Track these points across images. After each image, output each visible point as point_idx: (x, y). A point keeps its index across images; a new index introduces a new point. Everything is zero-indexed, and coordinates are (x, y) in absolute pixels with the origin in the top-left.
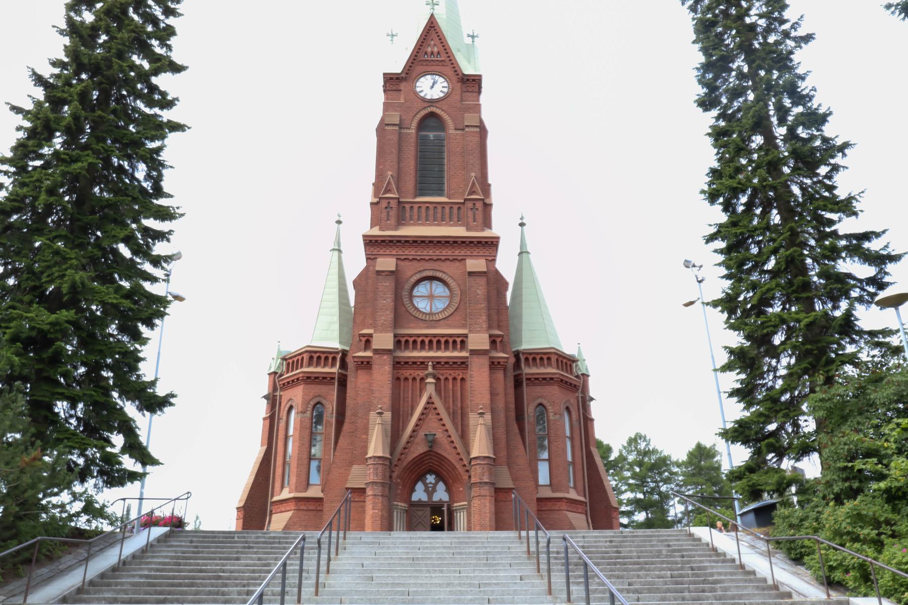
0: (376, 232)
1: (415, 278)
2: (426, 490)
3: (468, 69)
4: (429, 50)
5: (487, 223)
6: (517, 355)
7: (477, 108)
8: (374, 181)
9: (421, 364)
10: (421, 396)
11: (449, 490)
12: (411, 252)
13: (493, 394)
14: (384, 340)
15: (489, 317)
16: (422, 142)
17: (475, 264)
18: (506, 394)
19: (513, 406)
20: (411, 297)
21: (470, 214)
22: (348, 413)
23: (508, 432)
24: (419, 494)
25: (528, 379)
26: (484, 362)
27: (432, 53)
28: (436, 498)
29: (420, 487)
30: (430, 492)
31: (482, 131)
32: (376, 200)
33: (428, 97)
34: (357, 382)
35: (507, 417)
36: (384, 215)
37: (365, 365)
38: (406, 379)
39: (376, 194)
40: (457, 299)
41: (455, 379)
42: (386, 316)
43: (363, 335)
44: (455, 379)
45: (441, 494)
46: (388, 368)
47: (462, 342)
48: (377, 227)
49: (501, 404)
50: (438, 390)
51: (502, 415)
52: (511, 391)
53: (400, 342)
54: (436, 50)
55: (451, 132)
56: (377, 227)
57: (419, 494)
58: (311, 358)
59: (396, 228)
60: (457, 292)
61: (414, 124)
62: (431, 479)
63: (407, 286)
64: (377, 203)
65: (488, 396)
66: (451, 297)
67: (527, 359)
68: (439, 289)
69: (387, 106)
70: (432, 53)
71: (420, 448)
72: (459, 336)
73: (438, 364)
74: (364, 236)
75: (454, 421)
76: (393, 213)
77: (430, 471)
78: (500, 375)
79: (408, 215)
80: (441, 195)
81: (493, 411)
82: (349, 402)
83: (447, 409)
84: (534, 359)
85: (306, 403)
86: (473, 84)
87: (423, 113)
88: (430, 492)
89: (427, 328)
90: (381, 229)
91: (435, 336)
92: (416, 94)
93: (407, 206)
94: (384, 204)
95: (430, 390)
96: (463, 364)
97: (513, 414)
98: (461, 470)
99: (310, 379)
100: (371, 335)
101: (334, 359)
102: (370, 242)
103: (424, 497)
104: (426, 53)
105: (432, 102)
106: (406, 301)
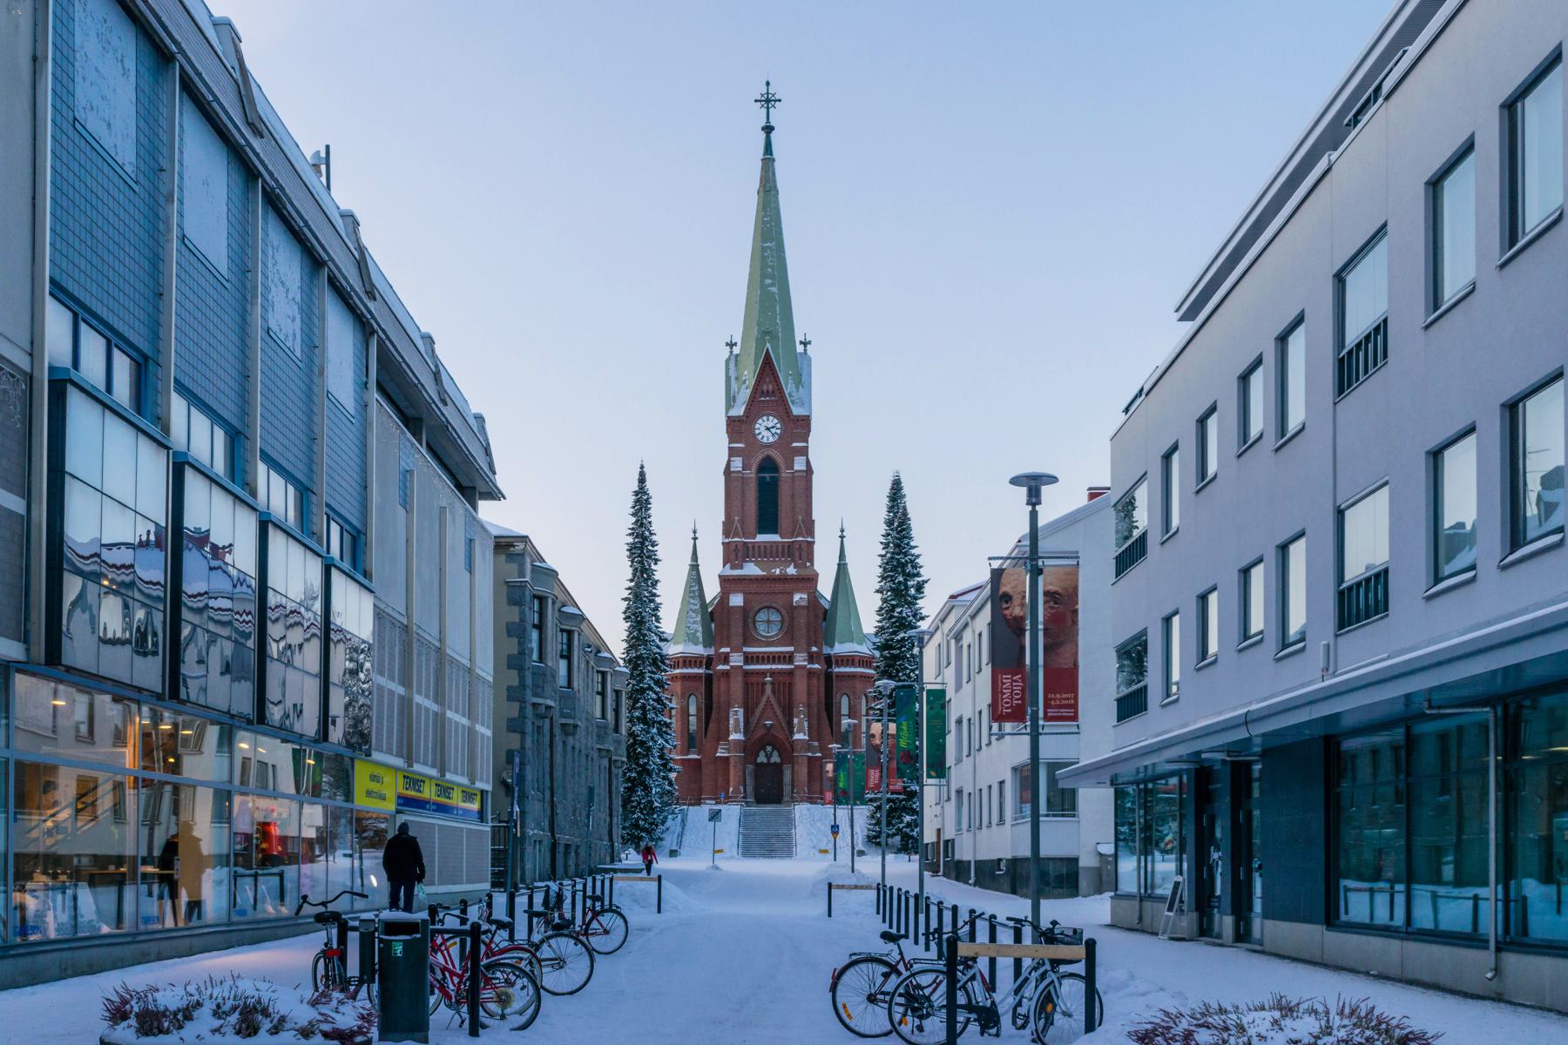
0: (729, 572)
1: (756, 609)
2: (766, 756)
3: (797, 411)
4: (765, 388)
5: (810, 558)
6: (828, 660)
7: (804, 452)
8: (723, 518)
9: (763, 673)
10: (762, 695)
11: (780, 756)
12: (754, 588)
13: (809, 694)
14: (737, 660)
15: (809, 638)
16: (762, 484)
17: (799, 598)
18: (818, 693)
19: (823, 700)
20: (754, 622)
21: (797, 554)
22: (715, 706)
23: (819, 720)
24: (762, 758)
25: (837, 676)
26: (805, 673)
27: (768, 392)
28: (772, 761)
29: (762, 754)
30: (769, 756)
31: (809, 471)
32: (727, 541)
33: (765, 440)
34: (719, 687)
35: (818, 709)
36: (733, 556)
37: (726, 674)
38: (752, 684)
39: (726, 533)
40: (786, 624)
41: (784, 683)
42: (737, 640)
43: (723, 653)
44: (784, 683)
45: (776, 759)
46: (740, 679)
47: (789, 658)
48: (728, 565)
49: (814, 701)
50: (773, 691)
51: (815, 710)
52: (822, 690)
53: (748, 659)
54: (771, 387)
55: (783, 475)
56: (728, 565)
57: (762, 758)
58: (685, 661)
59: (742, 568)
60: (787, 618)
61: (754, 468)
62: (769, 748)
63: (751, 615)
64: (729, 543)
65: (805, 696)
66: (782, 622)
67: (837, 660)
68: (775, 617)
69: (732, 452)
70: (768, 392)
71: (761, 732)
72: (787, 652)
73: (773, 673)
74: (720, 576)
75: (783, 712)
76: (740, 554)
77: (769, 745)
78: (815, 681)
79: (751, 553)
80: (775, 532)
81: (809, 706)
82: (715, 698)
83: (780, 704)
84: (842, 660)
85: (683, 695)
86: (799, 427)
87: (760, 457)
88: (769, 756)
89: (766, 646)
90: (731, 568)
91: (771, 653)
92: (755, 436)
93: (750, 546)
94: (733, 548)
95: (768, 689)
96: (791, 673)
97: (823, 707)
98: (788, 745)
99: (685, 677)
100: (728, 653)
101: (701, 662)
102: (724, 580)
103: (765, 761)
104: (763, 392)
105: (770, 446)
106: (751, 625)
